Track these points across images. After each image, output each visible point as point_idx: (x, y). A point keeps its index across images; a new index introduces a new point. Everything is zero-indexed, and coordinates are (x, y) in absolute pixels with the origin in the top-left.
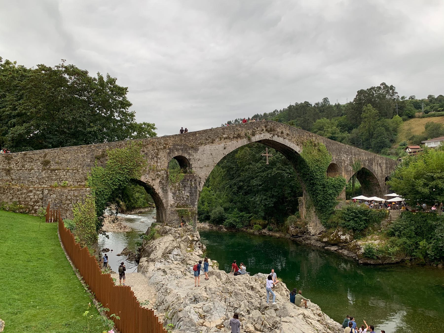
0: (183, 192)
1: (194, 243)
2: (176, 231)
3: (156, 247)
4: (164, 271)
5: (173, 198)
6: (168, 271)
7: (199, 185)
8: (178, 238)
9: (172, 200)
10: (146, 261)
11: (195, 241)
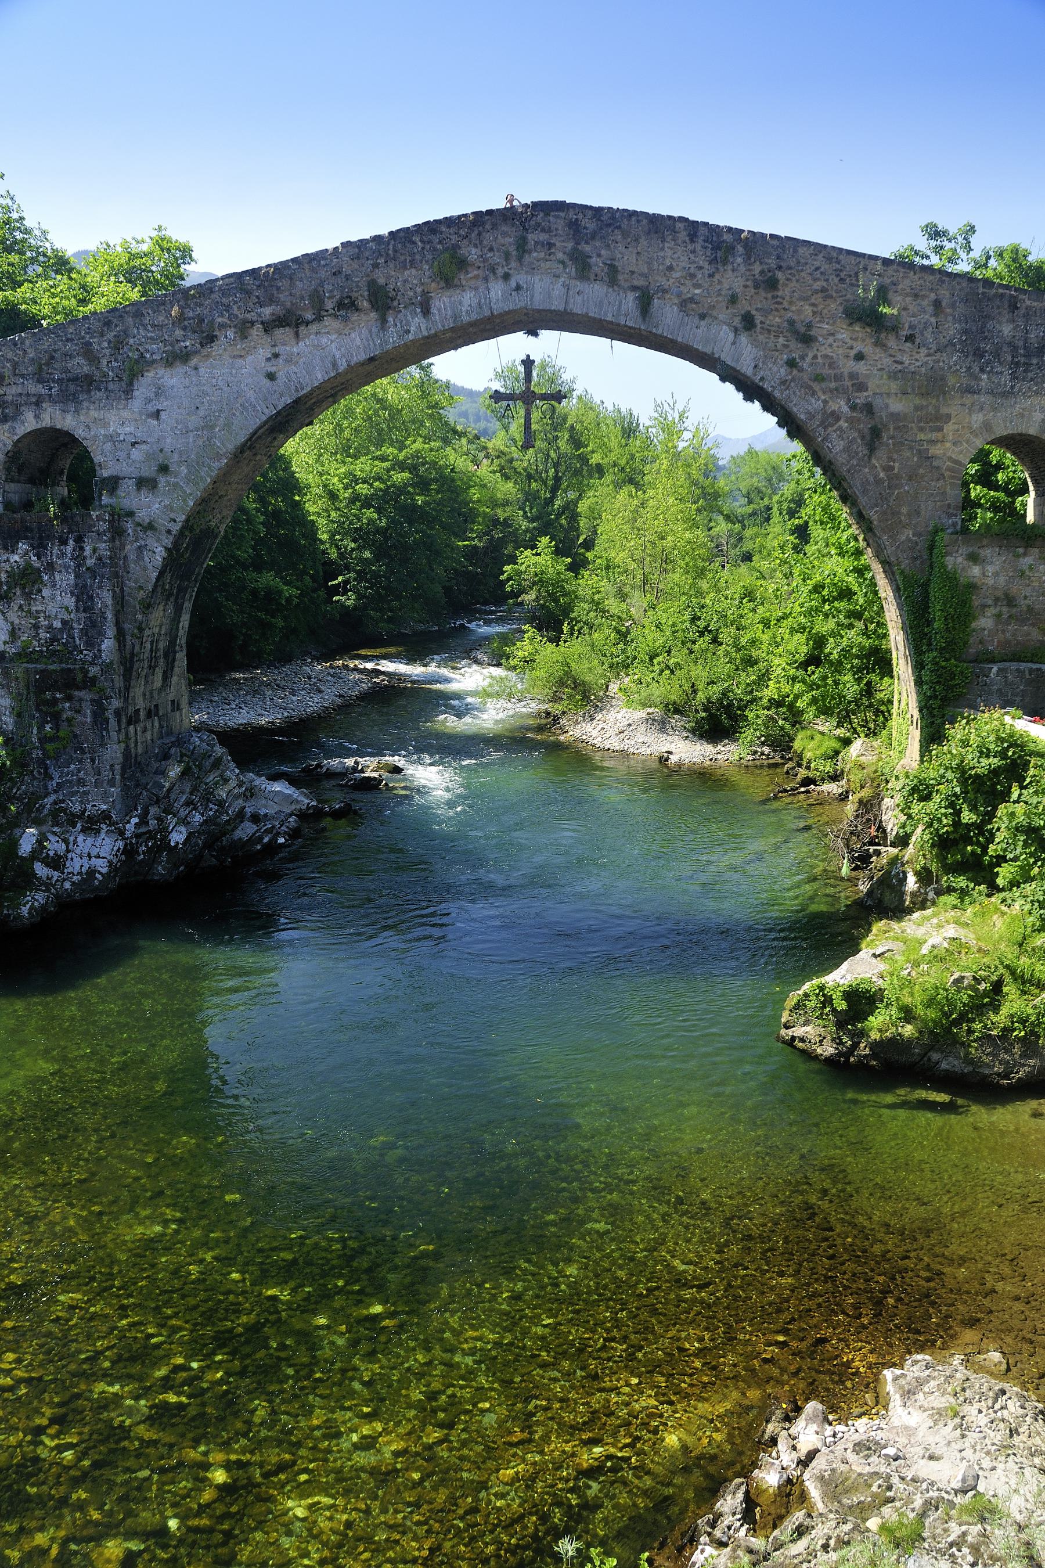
0: (46, 592)
7: (140, 557)
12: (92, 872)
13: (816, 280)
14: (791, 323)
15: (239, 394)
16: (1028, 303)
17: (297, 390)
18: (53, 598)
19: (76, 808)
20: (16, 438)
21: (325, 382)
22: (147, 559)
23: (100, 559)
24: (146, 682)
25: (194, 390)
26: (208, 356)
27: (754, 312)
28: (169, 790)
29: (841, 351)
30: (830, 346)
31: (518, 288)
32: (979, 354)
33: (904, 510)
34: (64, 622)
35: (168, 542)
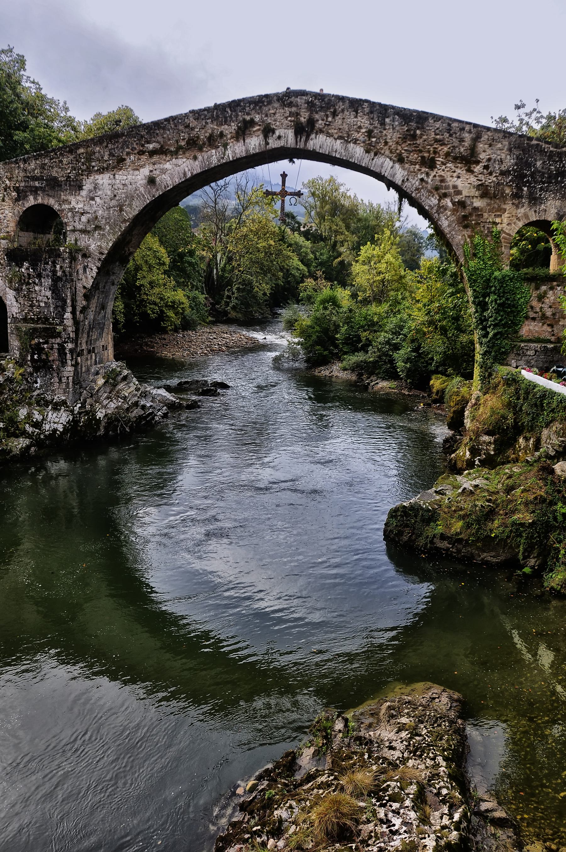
5: (17, 301)
9: (15, 303)
12: (55, 430)
13: (436, 134)
14: (423, 157)
16: (551, 149)
17: (165, 187)
18: (40, 291)
19: (49, 398)
20: (24, 209)
21: (180, 184)
22: (88, 273)
23: (64, 272)
24: (88, 336)
26: (121, 169)
27: (403, 151)
28: (98, 391)
29: (449, 173)
30: (443, 170)
31: (279, 137)
35: (99, 265)
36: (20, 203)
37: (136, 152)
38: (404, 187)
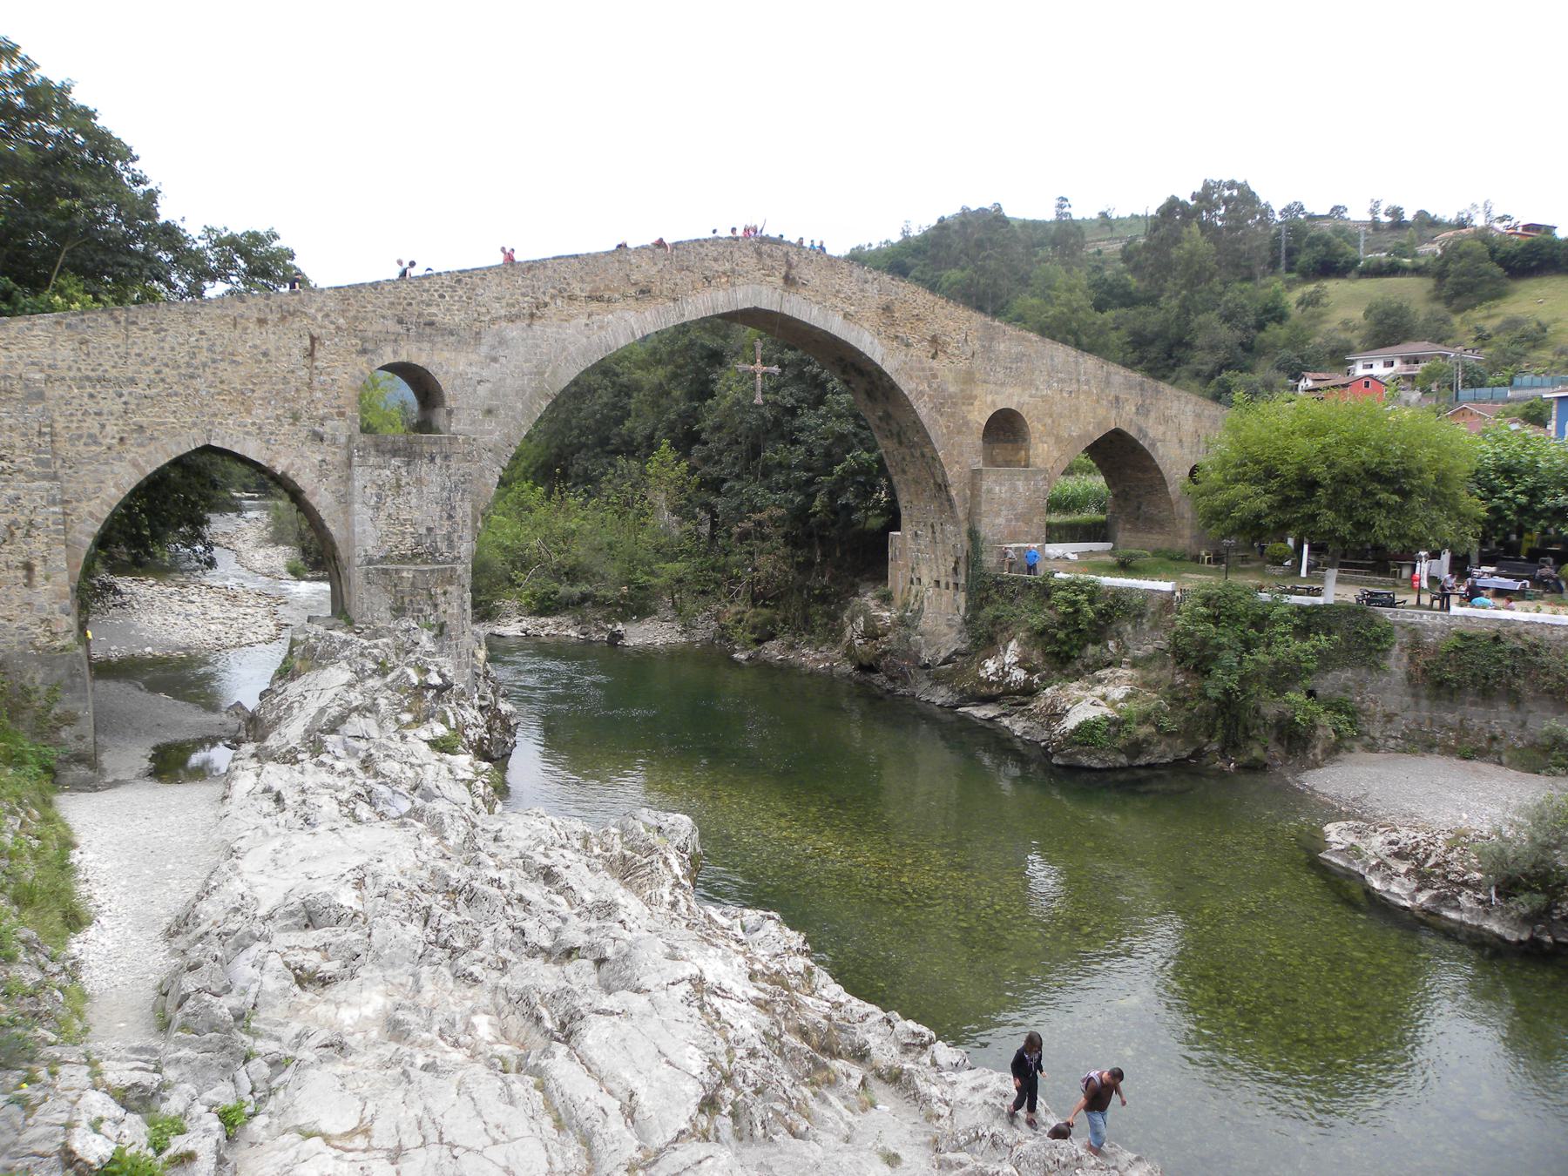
0: (414, 502)
1: (431, 694)
2: (366, 648)
3: (290, 708)
4: (279, 799)
6: (291, 798)
8: (370, 676)
10: (253, 755)
11: (435, 687)
15: (564, 349)
25: (530, 342)
32: (990, 359)
33: (955, 453)
34: (429, 530)
36: (364, 359)
37: (565, 294)
38: (884, 368)
